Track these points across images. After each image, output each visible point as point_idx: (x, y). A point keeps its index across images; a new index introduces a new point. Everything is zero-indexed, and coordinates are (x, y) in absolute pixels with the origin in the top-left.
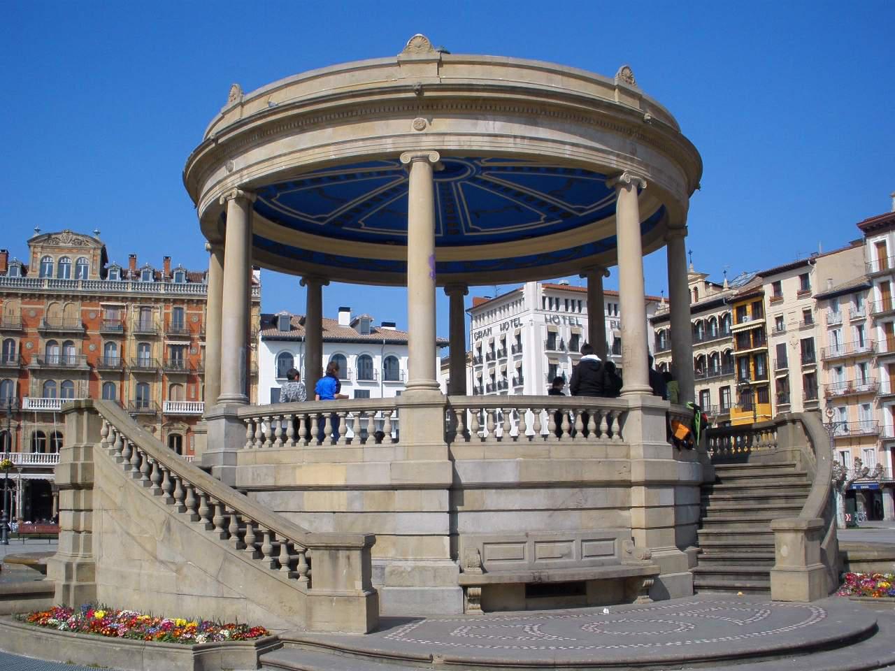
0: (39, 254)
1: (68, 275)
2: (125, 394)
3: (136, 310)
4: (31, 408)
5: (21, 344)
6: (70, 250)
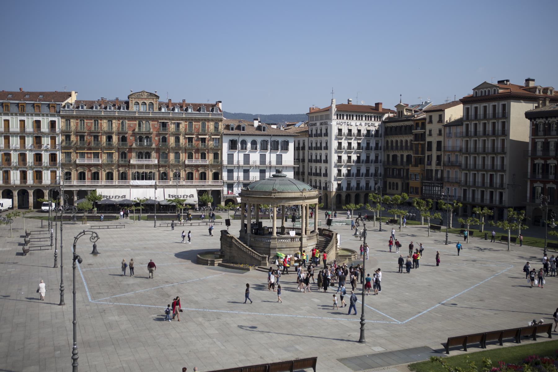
6: (145, 99)
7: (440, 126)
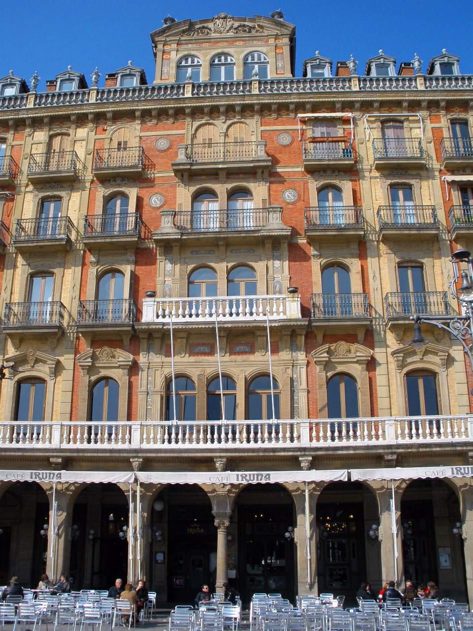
0: (173, 54)
2: (373, 284)
3: (374, 125)
4: (161, 320)
5: (139, 201)
6: (231, 41)
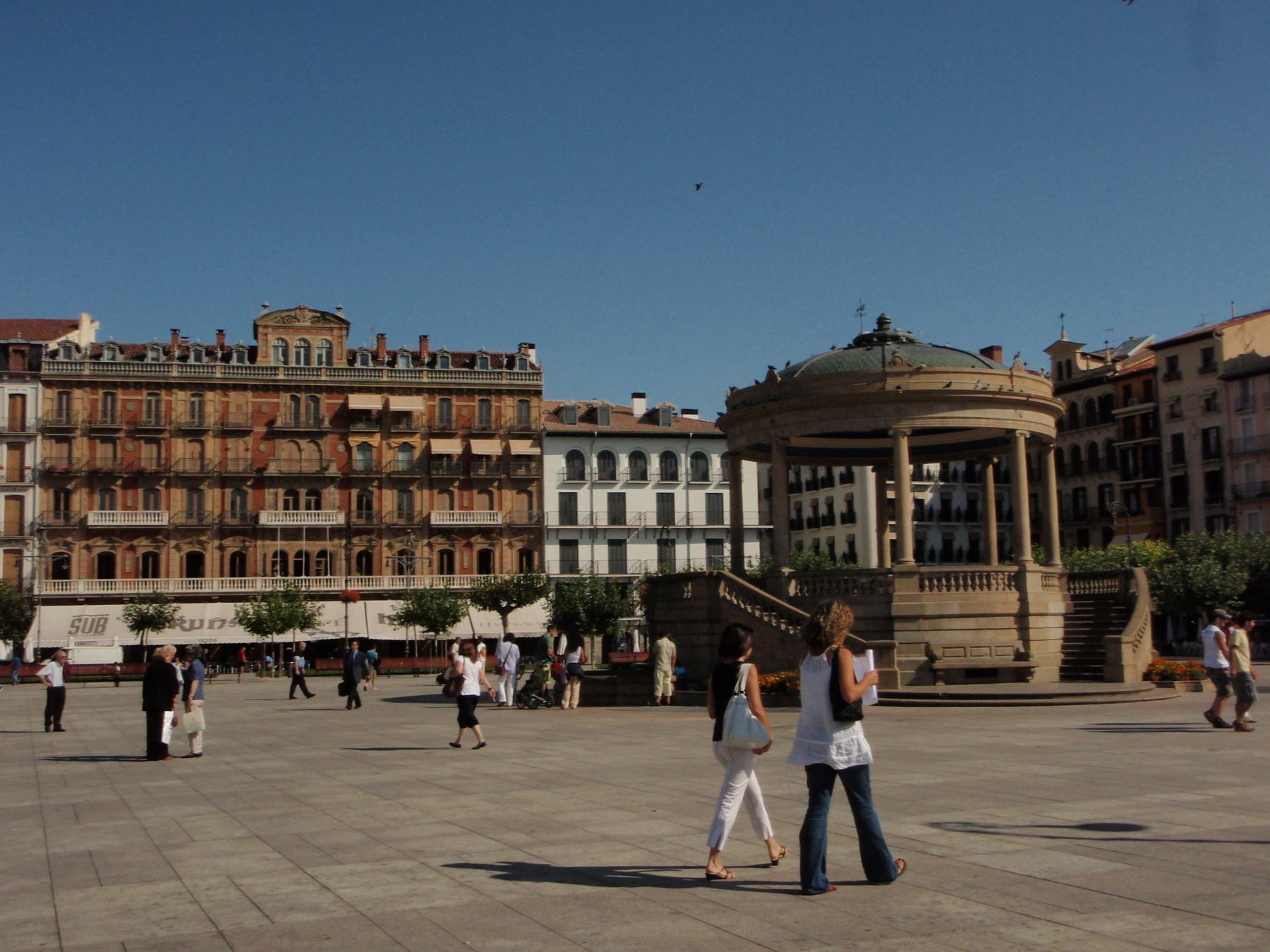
1: (298, 362)
6: (308, 330)
7: (1212, 382)
